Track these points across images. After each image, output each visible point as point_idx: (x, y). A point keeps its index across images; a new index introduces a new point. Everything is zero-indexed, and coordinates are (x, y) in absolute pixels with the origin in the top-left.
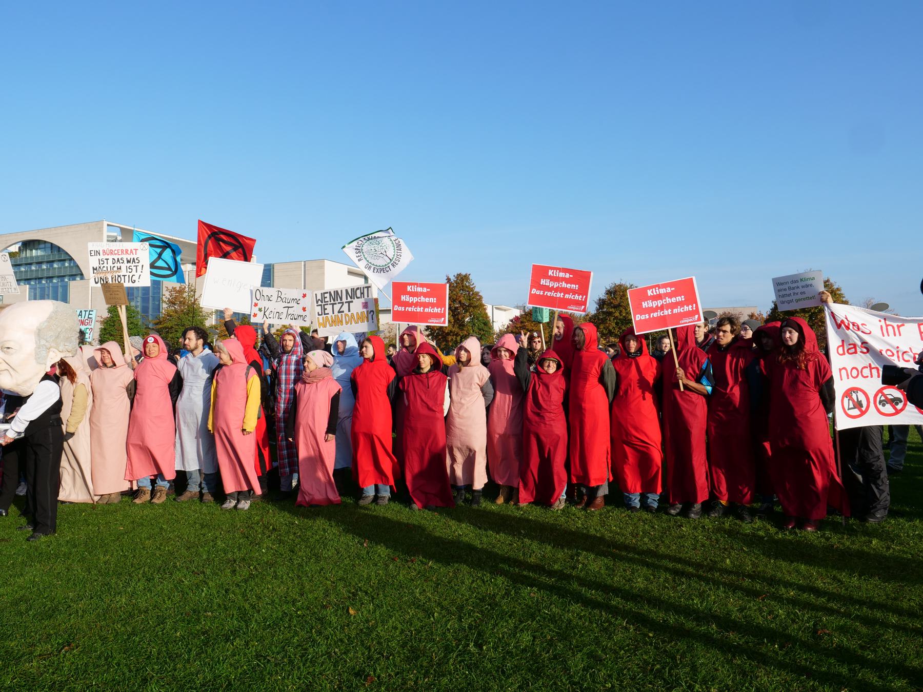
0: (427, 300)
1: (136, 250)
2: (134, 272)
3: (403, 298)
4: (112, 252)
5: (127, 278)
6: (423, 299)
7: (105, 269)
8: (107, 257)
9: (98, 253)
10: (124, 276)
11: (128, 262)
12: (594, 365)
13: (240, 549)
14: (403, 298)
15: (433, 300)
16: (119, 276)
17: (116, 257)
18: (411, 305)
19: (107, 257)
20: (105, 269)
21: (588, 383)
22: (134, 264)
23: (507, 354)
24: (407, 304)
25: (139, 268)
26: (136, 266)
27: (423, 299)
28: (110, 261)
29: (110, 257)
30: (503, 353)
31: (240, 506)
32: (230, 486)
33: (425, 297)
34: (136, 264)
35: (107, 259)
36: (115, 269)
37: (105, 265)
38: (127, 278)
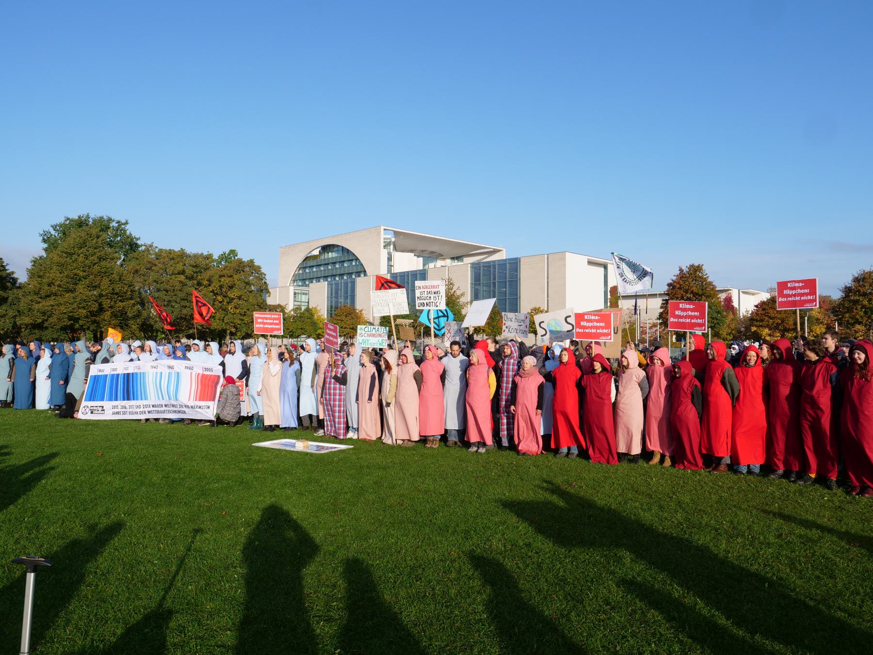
0: (598, 324)
1: (439, 285)
2: (437, 300)
3: (582, 323)
4: (426, 287)
5: (434, 303)
6: (595, 324)
7: (423, 298)
8: (424, 290)
9: (420, 287)
10: (432, 302)
11: (435, 293)
12: (718, 370)
13: (480, 472)
14: (582, 323)
15: (602, 324)
16: (430, 302)
17: (428, 290)
18: (587, 328)
19: (424, 290)
20: (423, 298)
21: (713, 383)
22: (437, 295)
23: (659, 362)
24: (584, 327)
25: (440, 297)
26: (438, 296)
27: (595, 324)
28: (426, 293)
29: (426, 290)
30: (656, 361)
31: (479, 451)
32: (474, 437)
33: (597, 322)
34: (439, 295)
35: (424, 292)
36: (428, 298)
37: (423, 295)
38: (434, 303)
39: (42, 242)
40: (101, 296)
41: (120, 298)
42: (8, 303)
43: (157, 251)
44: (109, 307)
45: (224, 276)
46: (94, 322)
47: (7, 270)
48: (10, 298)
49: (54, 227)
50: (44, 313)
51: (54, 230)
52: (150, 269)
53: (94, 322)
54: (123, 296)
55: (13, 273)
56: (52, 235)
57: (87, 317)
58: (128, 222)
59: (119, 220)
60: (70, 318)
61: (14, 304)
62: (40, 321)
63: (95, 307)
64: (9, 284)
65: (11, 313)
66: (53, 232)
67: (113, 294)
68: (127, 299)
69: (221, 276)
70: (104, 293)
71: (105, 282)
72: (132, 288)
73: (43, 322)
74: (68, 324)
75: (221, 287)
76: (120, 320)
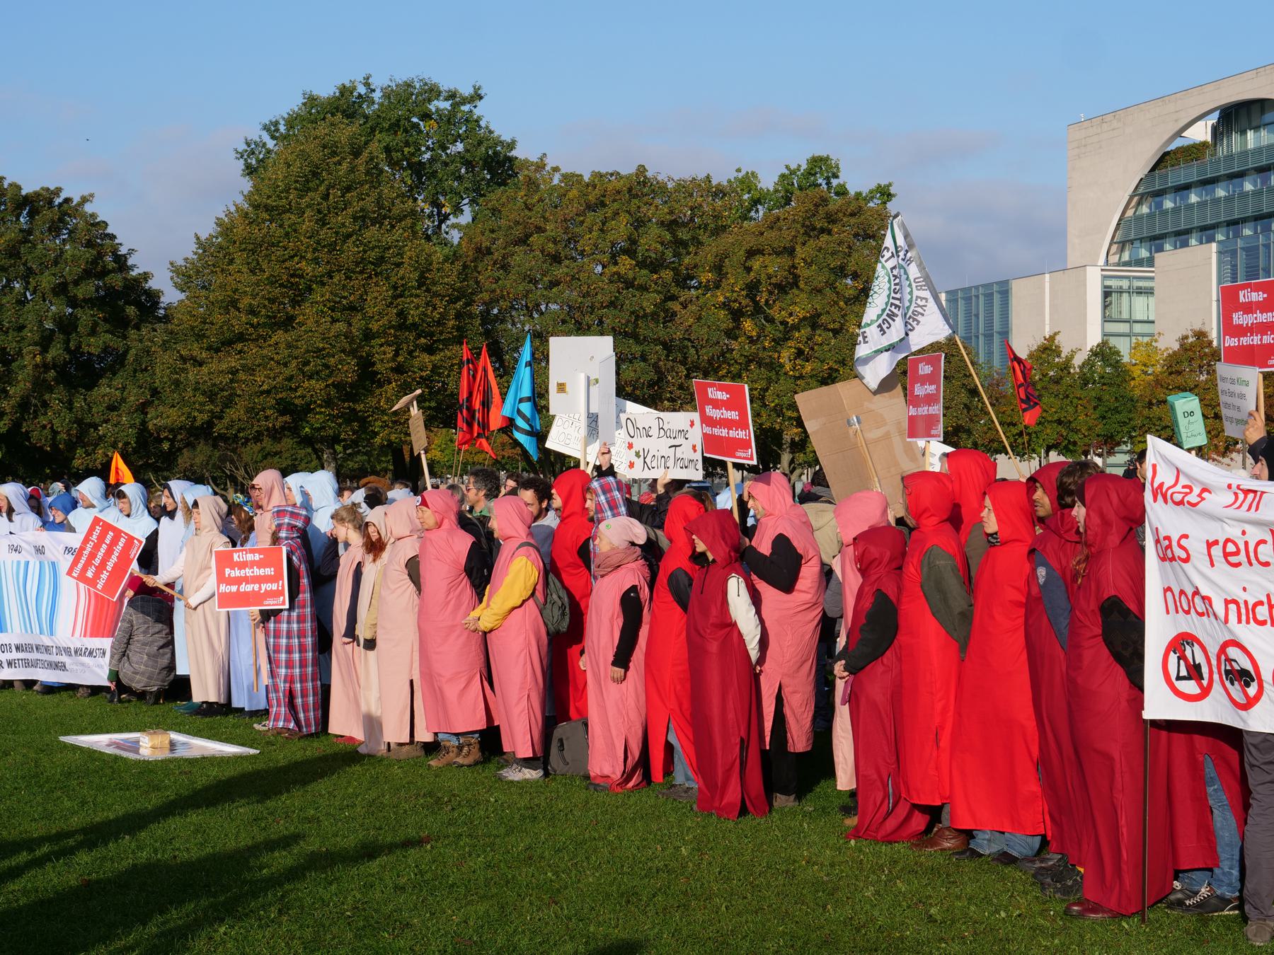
39: (242, 175)
40: (368, 335)
41: (423, 340)
42: (129, 368)
43: (556, 181)
44: (392, 369)
45: (760, 252)
46: (352, 416)
47: (132, 268)
48: (133, 352)
49: (272, 128)
50: (211, 396)
51: (273, 137)
52: (523, 241)
53: (352, 416)
54: (431, 335)
55: (146, 276)
56: (269, 151)
57: (328, 403)
58: (482, 92)
59: (452, 88)
60: (285, 407)
61: (142, 371)
62: (201, 418)
63: (348, 371)
64: (131, 311)
65: (134, 397)
66: (271, 144)
67: (402, 327)
68: (447, 343)
69: (751, 253)
70: (375, 327)
71: (379, 293)
72: (459, 305)
73: (210, 424)
74: (278, 425)
75: (752, 288)
76: (430, 408)
